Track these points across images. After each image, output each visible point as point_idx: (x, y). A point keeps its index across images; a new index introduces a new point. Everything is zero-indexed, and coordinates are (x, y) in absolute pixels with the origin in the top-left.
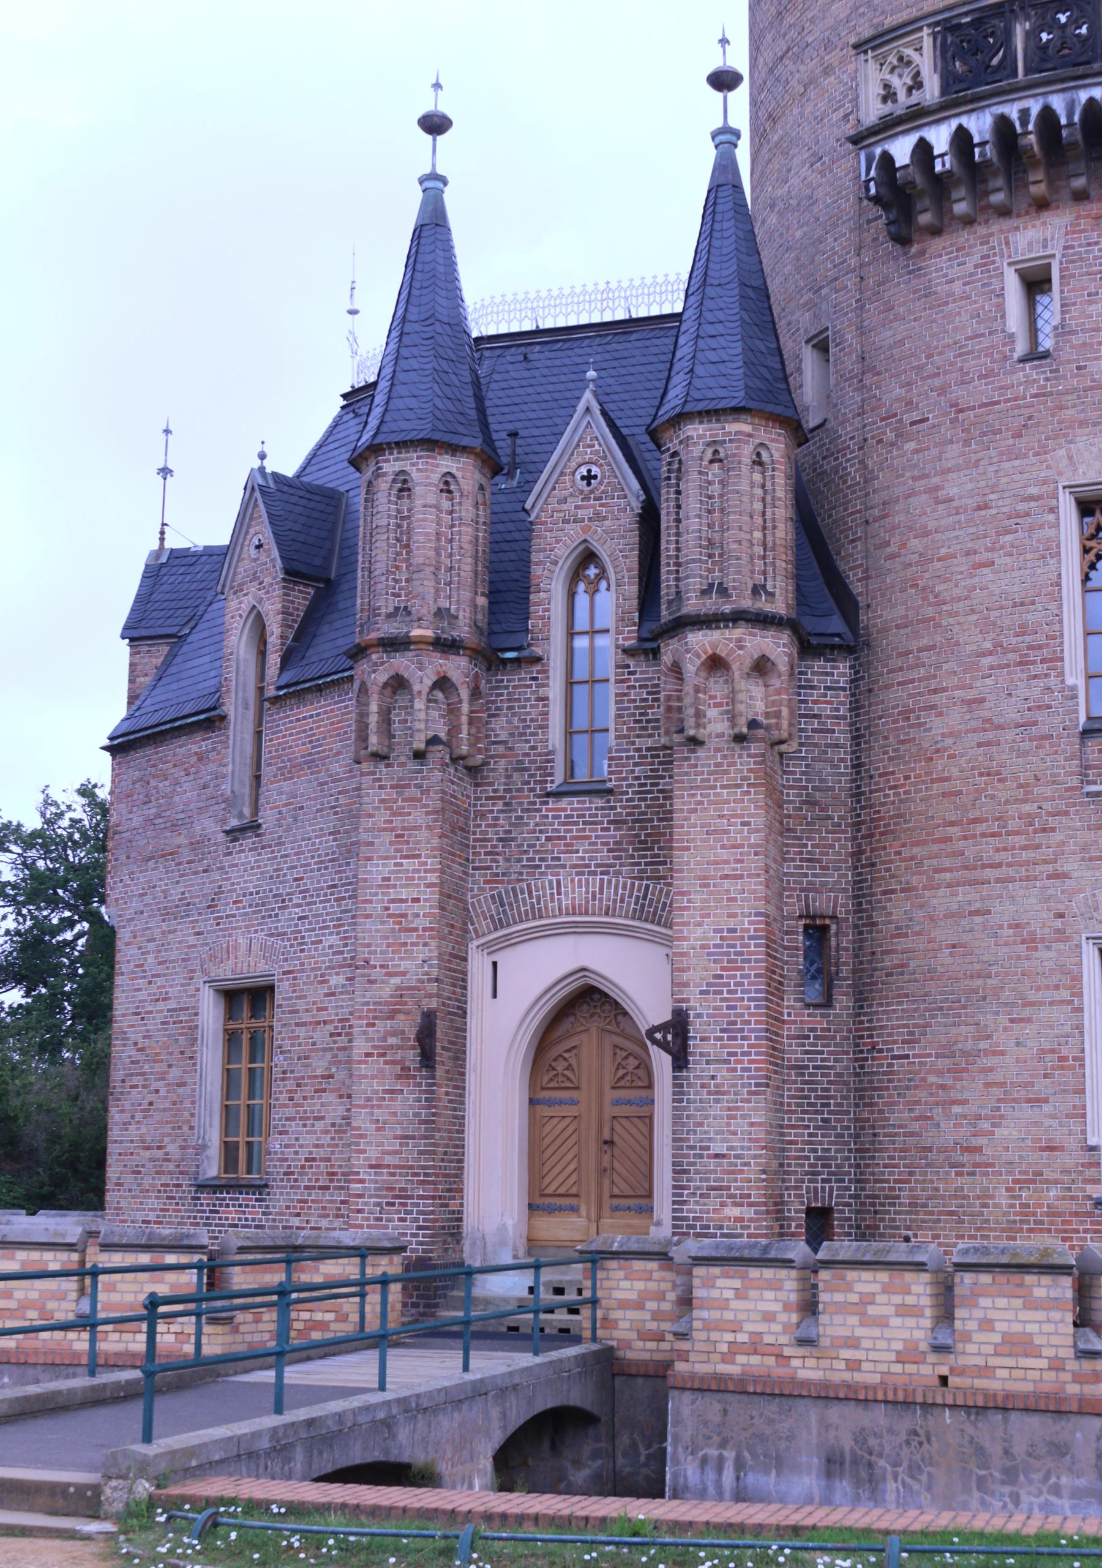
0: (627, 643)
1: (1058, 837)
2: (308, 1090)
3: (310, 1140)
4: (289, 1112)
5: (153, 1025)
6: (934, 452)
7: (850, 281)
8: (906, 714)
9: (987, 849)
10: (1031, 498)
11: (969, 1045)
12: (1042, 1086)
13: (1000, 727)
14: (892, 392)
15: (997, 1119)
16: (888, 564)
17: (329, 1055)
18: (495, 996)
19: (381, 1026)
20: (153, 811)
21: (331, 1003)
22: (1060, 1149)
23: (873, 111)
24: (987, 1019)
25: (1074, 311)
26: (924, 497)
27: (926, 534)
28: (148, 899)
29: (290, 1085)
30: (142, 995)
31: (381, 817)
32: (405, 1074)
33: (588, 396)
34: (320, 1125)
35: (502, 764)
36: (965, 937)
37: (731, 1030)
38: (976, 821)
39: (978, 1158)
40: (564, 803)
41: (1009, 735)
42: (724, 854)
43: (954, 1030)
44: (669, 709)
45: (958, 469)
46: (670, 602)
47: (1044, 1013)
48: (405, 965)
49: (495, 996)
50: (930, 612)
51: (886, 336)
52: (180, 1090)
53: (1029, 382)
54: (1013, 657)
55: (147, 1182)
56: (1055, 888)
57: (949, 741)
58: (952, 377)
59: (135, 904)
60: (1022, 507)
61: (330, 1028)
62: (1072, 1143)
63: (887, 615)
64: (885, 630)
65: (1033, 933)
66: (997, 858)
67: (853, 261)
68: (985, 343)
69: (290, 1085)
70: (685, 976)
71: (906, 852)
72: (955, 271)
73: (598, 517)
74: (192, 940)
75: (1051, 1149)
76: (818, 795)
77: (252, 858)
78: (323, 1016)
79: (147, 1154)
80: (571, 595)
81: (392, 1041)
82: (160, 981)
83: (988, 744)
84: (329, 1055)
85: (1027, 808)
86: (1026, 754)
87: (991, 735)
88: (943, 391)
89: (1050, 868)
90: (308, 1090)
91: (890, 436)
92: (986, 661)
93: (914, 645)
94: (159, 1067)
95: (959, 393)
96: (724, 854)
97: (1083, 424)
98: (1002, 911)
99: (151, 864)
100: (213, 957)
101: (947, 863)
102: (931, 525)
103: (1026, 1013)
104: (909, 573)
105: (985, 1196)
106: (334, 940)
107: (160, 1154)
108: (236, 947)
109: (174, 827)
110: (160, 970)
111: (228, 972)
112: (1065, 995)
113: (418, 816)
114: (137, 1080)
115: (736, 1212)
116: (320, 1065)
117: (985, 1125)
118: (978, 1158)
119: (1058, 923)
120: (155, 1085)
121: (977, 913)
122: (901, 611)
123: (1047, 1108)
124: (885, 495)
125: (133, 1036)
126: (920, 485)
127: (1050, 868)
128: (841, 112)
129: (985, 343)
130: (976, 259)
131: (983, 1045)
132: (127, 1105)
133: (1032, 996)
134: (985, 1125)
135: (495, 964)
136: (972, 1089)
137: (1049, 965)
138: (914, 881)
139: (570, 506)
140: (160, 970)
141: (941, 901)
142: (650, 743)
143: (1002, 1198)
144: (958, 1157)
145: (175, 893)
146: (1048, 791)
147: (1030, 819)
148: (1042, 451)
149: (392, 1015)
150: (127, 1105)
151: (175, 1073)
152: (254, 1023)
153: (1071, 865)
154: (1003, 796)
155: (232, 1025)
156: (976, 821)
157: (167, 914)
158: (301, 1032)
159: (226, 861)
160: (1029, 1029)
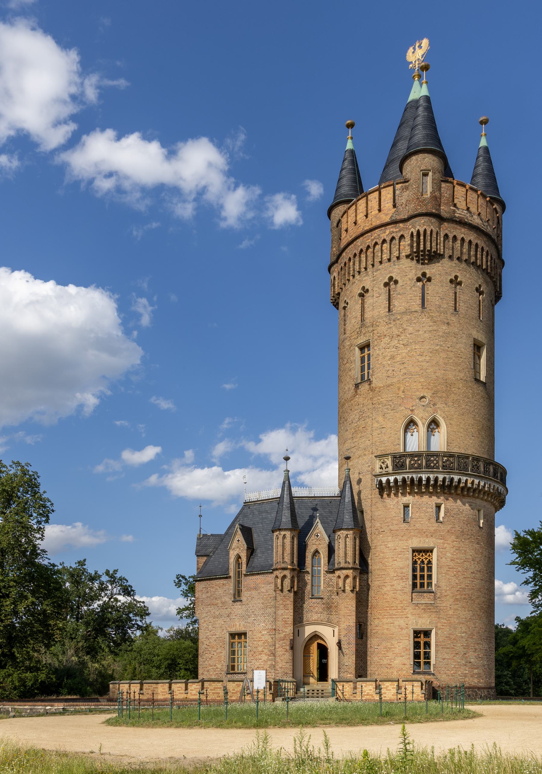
0: (326, 570)
1: (407, 610)
2: (257, 654)
3: (259, 663)
4: (252, 658)
5: (211, 640)
6: (386, 538)
7: (369, 501)
8: (379, 586)
9: (394, 612)
10: (404, 549)
11: (390, 646)
12: (403, 654)
13: (397, 590)
14: (378, 525)
15: (395, 659)
16: (376, 558)
17: (263, 647)
18: (298, 636)
19: (281, 642)
20: (209, 595)
21: (263, 637)
22: (406, 664)
23: (378, 471)
24: (393, 642)
25: (414, 514)
26: (384, 546)
27: (384, 553)
28: (209, 614)
29: (252, 653)
30: (207, 634)
31: (281, 602)
32: (286, 651)
33: (318, 519)
34: (260, 661)
35: (300, 592)
36: (389, 628)
37: (349, 644)
38: (392, 607)
39: (391, 666)
40: (313, 600)
41: (399, 592)
42: (348, 612)
43: (387, 644)
44: (337, 584)
45: (391, 541)
46: (338, 564)
47: (404, 641)
48: (286, 630)
49: (298, 636)
50: (384, 568)
51: (377, 514)
52: (221, 654)
53: (405, 527)
54: (400, 578)
55: (211, 673)
56: (406, 620)
57: (387, 592)
58: (390, 524)
59: (204, 615)
60: (402, 550)
61: (263, 642)
62: (408, 663)
63: (375, 567)
64: (375, 570)
65: (402, 627)
66: (397, 613)
67: (370, 497)
68: (397, 518)
69: (252, 653)
70: (341, 634)
71: (378, 612)
72: (391, 503)
73: (320, 544)
74: (223, 623)
75: (404, 664)
76: (361, 600)
77: (240, 607)
78: (261, 639)
79: (211, 667)
80: (313, 558)
81: (283, 644)
82: (214, 631)
83: (395, 593)
84: (263, 647)
85: (401, 605)
86: (402, 595)
87: (395, 592)
88: (388, 526)
89: (405, 616)
90: (257, 654)
91: (377, 533)
92: (395, 578)
93: (381, 574)
94: (213, 649)
95: (391, 527)
96: (348, 612)
97: (414, 536)
98: (397, 623)
99: (210, 606)
100: (229, 627)
101: (386, 614)
102: (385, 552)
103: (401, 641)
104: (380, 560)
105: (392, 673)
106: (263, 624)
107: (215, 667)
108: (236, 625)
109: (216, 599)
110: (213, 629)
111: (233, 630)
112: (407, 638)
113: (288, 602)
114: (207, 652)
115: (349, 675)
116: (260, 649)
117: (393, 660)
118: (391, 666)
119: (407, 626)
120: (212, 653)
121: (392, 623)
122: (378, 567)
123: (404, 657)
124: (375, 544)
125: (205, 643)
126: (383, 544)
127: (405, 616)
128: (368, 465)
129: (397, 518)
130: (396, 501)
131: (392, 646)
132: (204, 657)
133: (401, 638)
134: (393, 660)
135: (298, 630)
136: (390, 654)
137: (405, 633)
138: (380, 617)
139: (314, 541)
140: (213, 629)
141: (385, 621)
142: (330, 589)
143: (395, 673)
144: (387, 666)
145: (217, 613)
146: (406, 602)
147: (402, 607)
148: (407, 540)
149: (284, 640)
150: (204, 657)
151: (219, 651)
152: (239, 640)
153: (409, 616)
154: (397, 603)
155: (232, 641)
156: (392, 607)
157: (214, 617)
158: (255, 642)
159: (232, 607)
160: (401, 644)
